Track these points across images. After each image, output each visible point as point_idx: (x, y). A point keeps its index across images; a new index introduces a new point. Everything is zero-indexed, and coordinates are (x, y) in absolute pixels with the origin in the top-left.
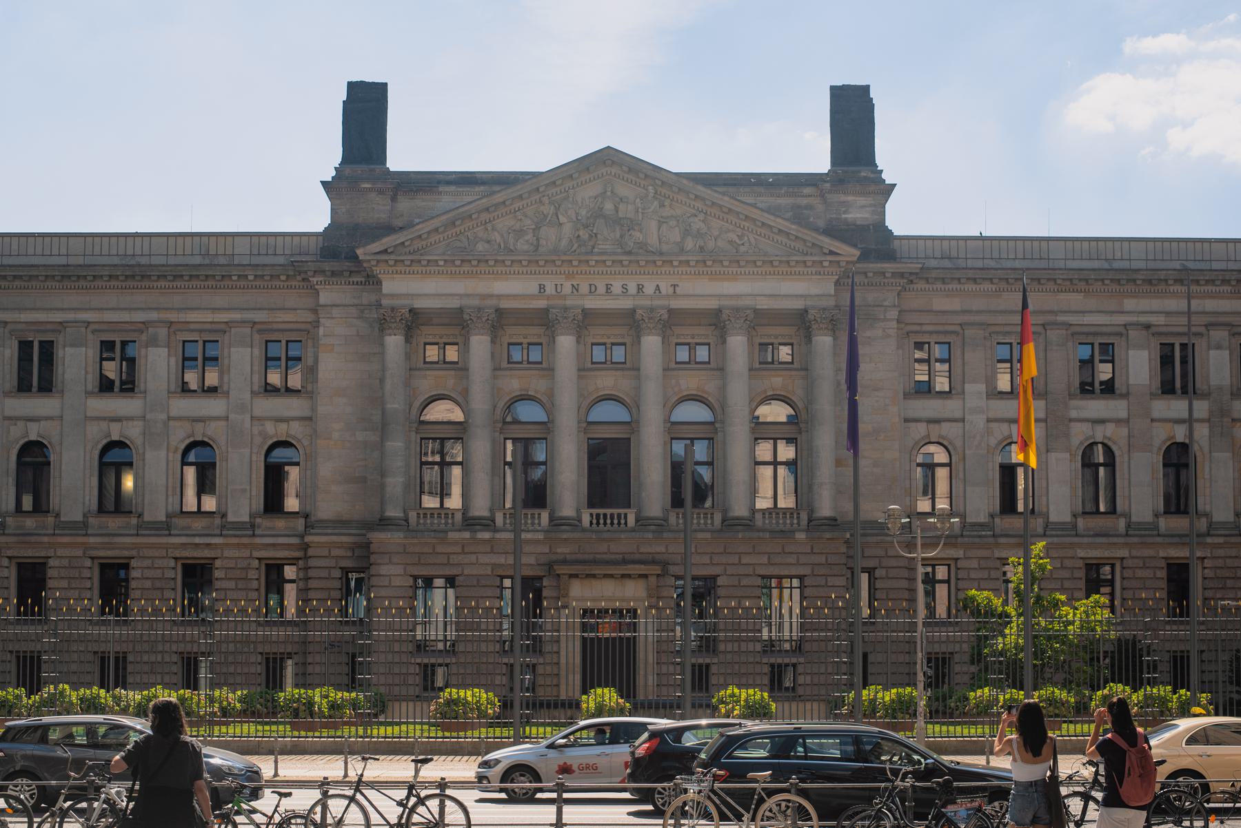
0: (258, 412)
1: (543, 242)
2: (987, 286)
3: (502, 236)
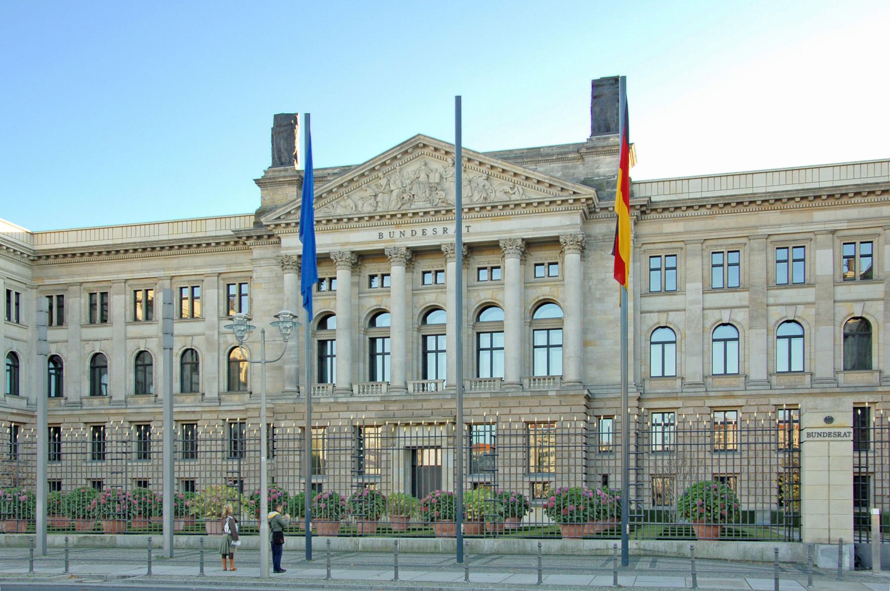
1: (380, 204)
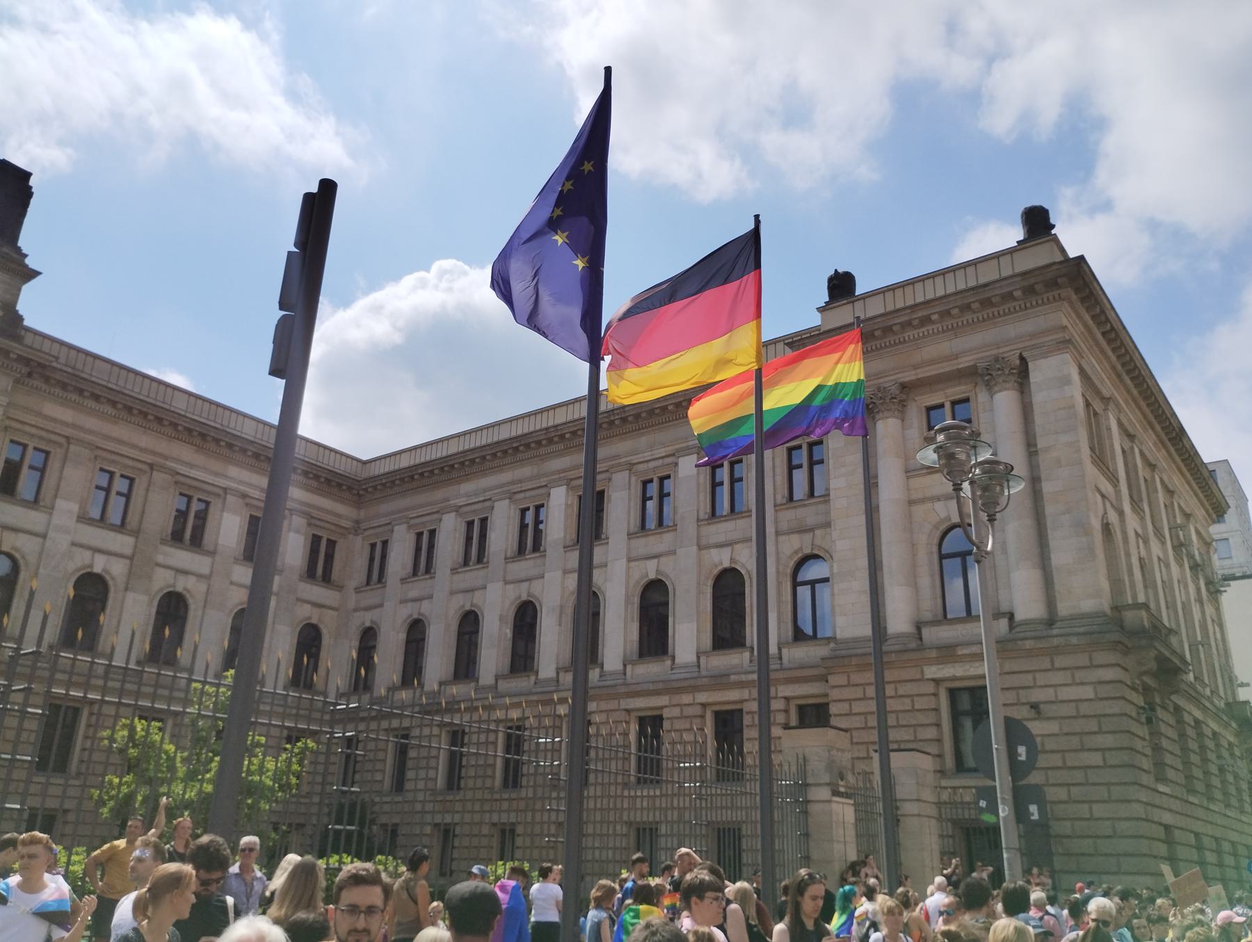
2: (108, 409)
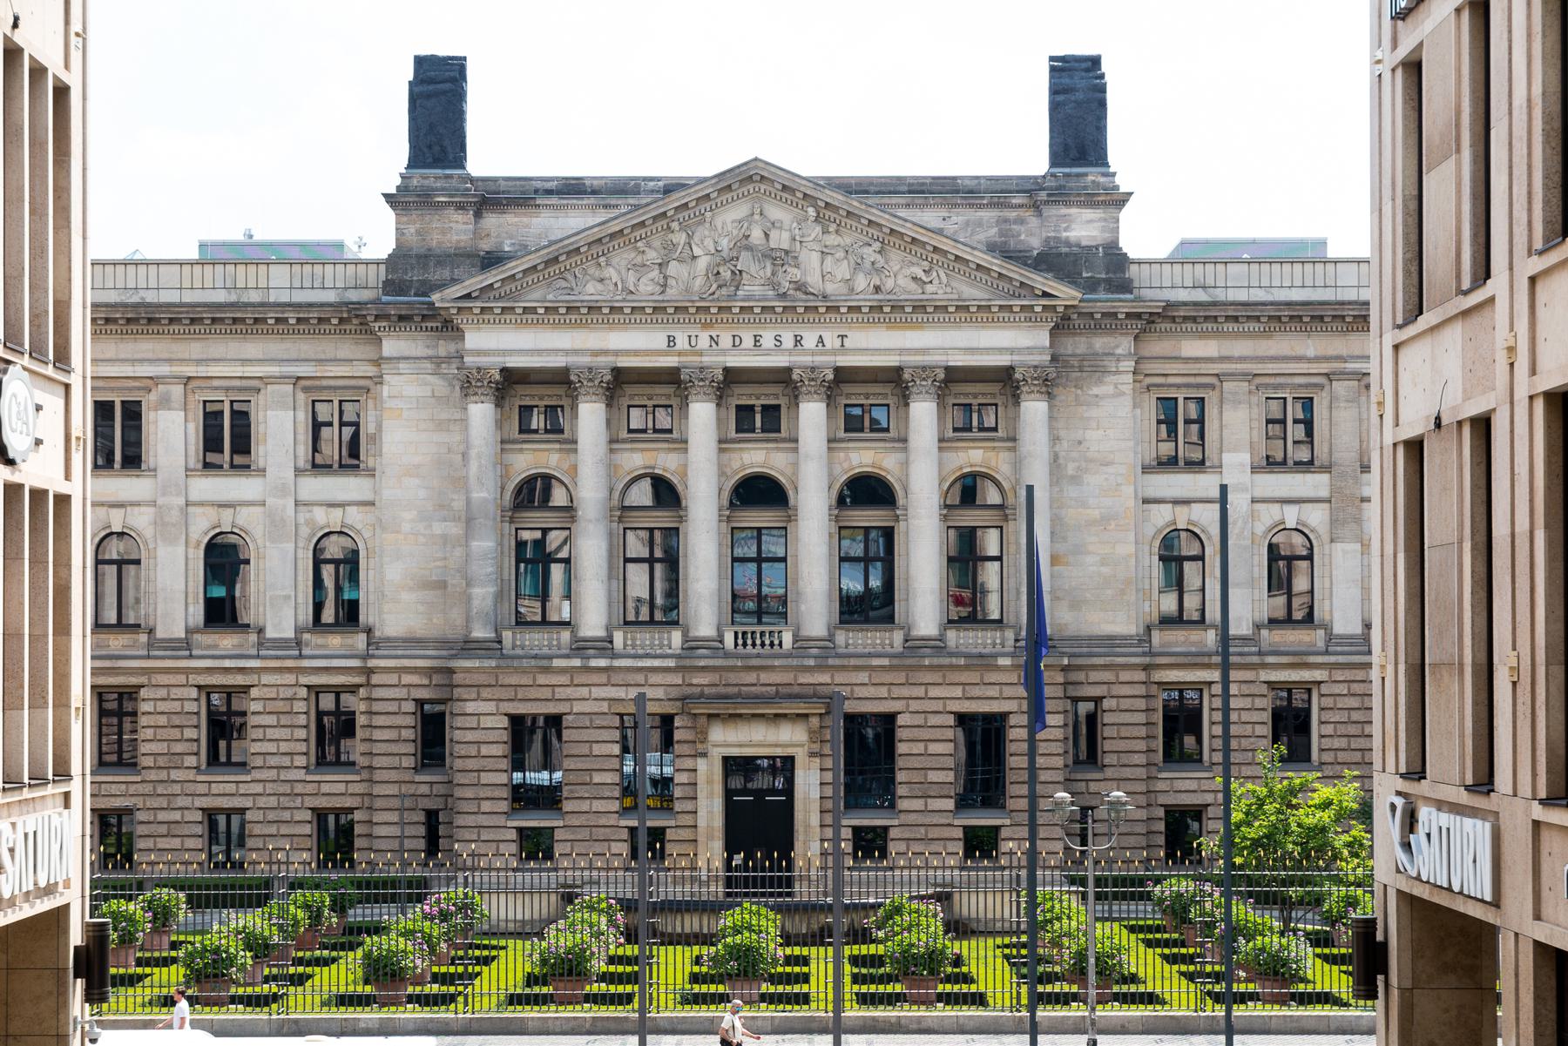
0: (304, 495)
1: (671, 282)
2: (1253, 326)
3: (619, 272)
